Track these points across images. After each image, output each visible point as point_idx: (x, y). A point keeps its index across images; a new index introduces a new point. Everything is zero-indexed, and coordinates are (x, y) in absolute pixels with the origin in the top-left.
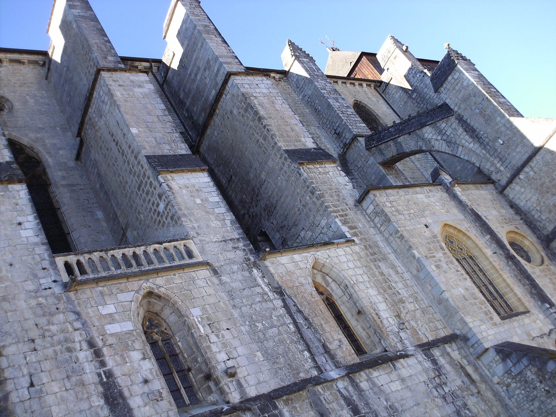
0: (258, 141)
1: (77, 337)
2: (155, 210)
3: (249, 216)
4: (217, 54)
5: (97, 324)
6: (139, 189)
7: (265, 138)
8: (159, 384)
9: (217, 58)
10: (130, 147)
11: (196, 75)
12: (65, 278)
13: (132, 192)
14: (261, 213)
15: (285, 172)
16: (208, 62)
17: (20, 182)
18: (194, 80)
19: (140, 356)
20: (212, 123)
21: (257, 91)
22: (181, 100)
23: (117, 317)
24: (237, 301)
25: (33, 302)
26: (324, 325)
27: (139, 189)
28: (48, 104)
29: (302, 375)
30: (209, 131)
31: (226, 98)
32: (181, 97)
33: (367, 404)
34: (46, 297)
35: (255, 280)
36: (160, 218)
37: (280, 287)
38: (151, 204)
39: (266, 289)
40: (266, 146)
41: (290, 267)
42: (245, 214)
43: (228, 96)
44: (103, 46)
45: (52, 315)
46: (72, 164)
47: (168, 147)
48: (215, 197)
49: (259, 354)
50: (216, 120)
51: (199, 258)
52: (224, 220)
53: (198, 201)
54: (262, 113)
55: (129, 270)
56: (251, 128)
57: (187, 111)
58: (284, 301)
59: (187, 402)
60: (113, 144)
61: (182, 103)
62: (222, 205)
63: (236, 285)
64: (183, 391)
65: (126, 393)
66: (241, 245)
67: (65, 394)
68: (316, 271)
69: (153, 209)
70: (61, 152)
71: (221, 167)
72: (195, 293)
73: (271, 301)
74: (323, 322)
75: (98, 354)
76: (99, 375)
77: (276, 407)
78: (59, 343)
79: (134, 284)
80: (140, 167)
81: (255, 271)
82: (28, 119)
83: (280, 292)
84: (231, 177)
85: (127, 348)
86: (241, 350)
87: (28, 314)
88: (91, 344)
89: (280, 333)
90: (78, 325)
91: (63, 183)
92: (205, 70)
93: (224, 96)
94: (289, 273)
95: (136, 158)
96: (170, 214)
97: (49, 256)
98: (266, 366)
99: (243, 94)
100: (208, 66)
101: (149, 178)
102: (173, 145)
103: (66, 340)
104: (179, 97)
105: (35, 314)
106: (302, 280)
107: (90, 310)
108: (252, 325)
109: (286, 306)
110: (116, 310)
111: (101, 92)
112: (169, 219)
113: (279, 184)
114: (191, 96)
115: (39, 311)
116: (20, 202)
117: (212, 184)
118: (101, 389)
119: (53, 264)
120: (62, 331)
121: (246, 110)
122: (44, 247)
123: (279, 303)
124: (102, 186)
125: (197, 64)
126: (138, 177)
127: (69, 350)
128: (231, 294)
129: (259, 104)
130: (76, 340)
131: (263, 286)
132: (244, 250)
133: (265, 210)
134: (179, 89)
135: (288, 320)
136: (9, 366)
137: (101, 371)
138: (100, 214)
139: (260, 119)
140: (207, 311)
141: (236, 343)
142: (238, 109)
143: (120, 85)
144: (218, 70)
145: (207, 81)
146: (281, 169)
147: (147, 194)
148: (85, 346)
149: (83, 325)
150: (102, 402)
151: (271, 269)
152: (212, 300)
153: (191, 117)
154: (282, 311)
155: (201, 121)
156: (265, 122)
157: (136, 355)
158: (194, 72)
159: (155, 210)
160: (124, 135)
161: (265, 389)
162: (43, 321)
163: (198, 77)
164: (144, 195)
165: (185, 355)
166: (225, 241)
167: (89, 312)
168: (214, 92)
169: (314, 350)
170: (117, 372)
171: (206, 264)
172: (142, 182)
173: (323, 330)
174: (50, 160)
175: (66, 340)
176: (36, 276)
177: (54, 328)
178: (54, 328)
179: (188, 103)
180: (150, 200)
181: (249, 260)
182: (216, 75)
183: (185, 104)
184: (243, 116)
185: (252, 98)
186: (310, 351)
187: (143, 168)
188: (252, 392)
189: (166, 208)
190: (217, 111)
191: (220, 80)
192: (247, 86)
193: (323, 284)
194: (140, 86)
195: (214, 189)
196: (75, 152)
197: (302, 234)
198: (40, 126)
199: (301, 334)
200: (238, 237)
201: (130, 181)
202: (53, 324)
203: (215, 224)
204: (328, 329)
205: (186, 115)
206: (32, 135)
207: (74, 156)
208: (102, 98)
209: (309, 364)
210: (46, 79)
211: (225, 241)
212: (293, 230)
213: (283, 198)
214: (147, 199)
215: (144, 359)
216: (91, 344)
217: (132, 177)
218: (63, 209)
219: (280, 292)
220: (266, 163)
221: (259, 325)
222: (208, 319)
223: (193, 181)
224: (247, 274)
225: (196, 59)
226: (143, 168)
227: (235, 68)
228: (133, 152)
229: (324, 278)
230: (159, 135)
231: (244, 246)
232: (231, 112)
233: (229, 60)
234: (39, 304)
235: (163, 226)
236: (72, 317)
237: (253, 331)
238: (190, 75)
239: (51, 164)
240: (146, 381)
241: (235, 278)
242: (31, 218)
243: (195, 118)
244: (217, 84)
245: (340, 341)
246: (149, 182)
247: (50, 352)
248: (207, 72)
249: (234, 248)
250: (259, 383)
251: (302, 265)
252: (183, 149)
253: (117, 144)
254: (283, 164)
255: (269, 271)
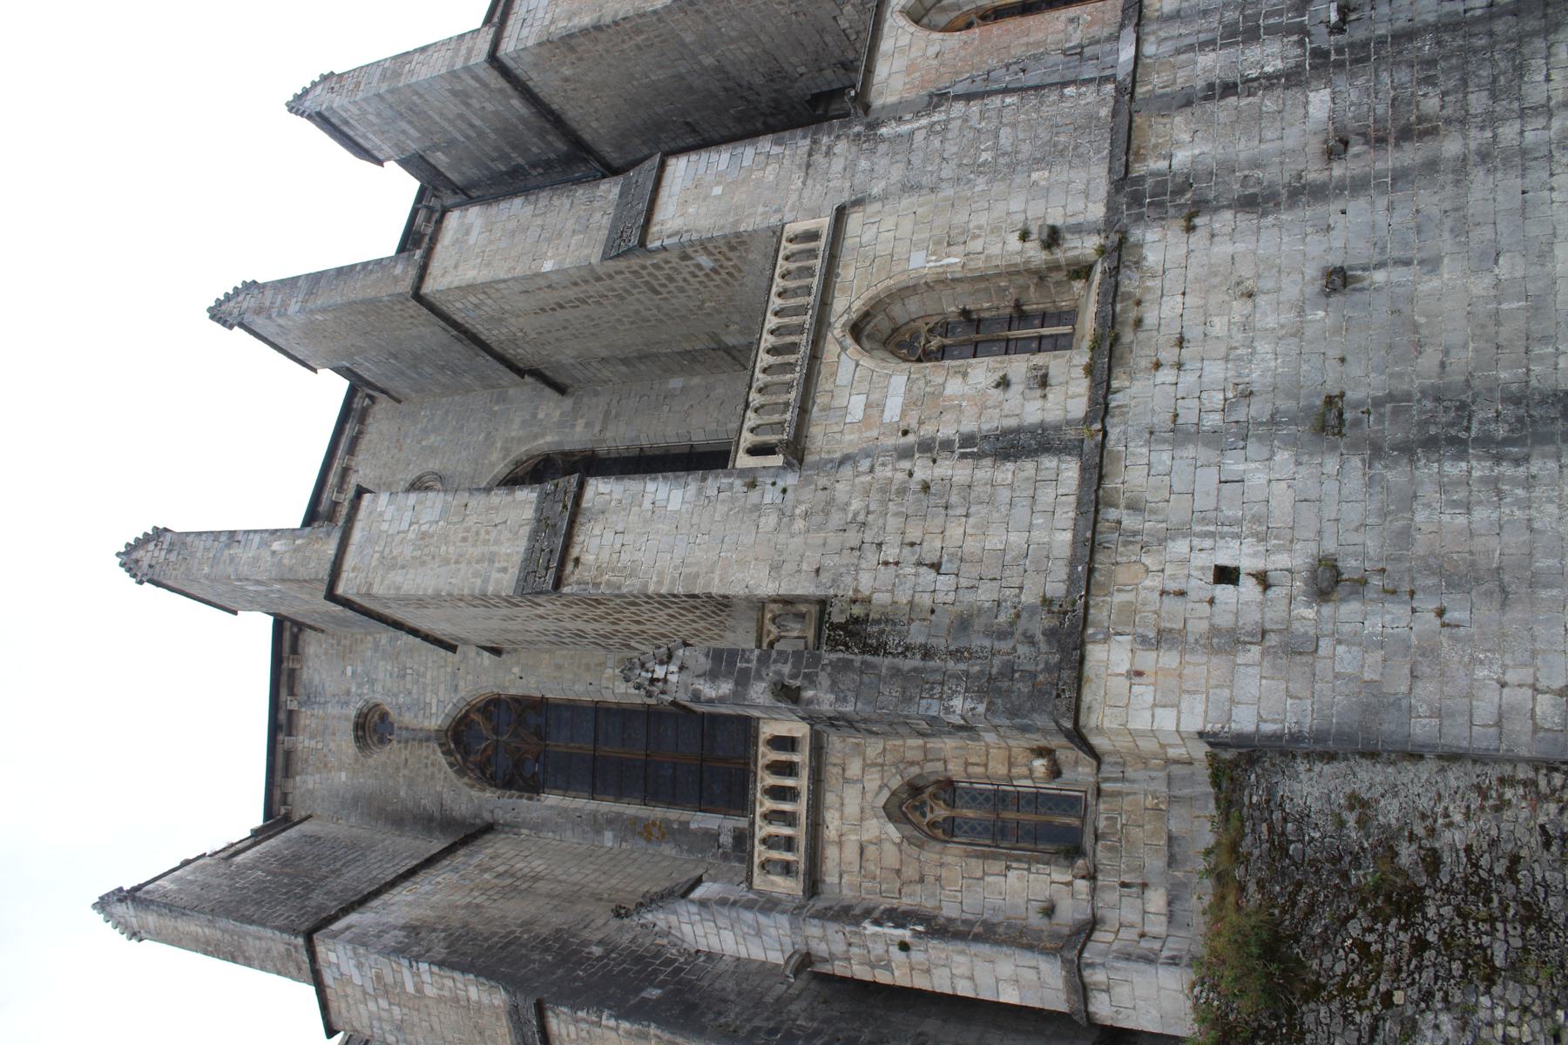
0: (638, 47)
1: (884, 473)
2: (707, 275)
3: (772, 115)
4: (444, 71)
5: (875, 433)
6: (658, 293)
7: (638, 31)
8: (1019, 366)
9: (453, 74)
10: (575, 284)
11: (472, 126)
12: (777, 460)
13: (659, 308)
14: (776, 91)
15: (716, 13)
16: (455, 93)
17: (581, 486)
18: (481, 134)
19: (959, 380)
20: (574, 125)
21: (540, 14)
22: (507, 173)
23: (875, 396)
24: (925, 180)
25: (799, 524)
26: (1031, 40)
27: (658, 293)
28: (447, 413)
29: (1104, 112)
30: (587, 136)
31: (538, 81)
32: (503, 169)
33: (1205, 13)
34: (799, 502)
35: (900, 135)
36: (723, 272)
37: (931, 96)
38: (692, 280)
39: (924, 121)
40: (652, 35)
41: (900, 63)
42: (765, 123)
43: (534, 75)
44: (374, 277)
45: (830, 502)
46: (568, 403)
47: (598, 215)
48: (721, 159)
49: (1035, 176)
50: (572, 114)
51: (824, 223)
52: (768, 155)
53: (718, 191)
54: (586, 20)
55: (804, 350)
56: (608, 51)
57: (534, 166)
58: (957, 97)
59: (1067, 329)
60: (559, 313)
61: (516, 172)
62: (740, 150)
63: (897, 173)
64: (1046, 331)
65: (1012, 422)
66: (825, 140)
67: (971, 520)
68: (925, 21)
69: (703, 279)
70: (541, 416)
71: (663, 136)
72: (883, 249)
73: (948, 121)
74: (1025, 40)
75: (926, 447)
76: (963, 456)
77: (1142, 178)
78: (884, 503)
79: (831, 349)
80: (618, 277)
81: (883, 130)
82: (464, 454)
83: (938, 99)
84: (687, 124)
85: (937, 395)
86: (1016, 204)
87: (817, 538)
88: (905, 453)
89: (1013, 125)
90: (865, 465)
91: (597, 428)
92: (468, 105)
93: (530, 84)
94: (910, 69)
95: (599, 279)
96: (725, 249)
97: (727, 476)
98: (1062, 173)
99: (540, 45)
100: (462, 96)
101: (644, 267)
102: (596, 204)
103: (883, 490)
104: (502, 174)
105: (821, 527)
106: (932, 51)
107: (847, 438)
108: (979, 169)
109: (968, 97)
110: (866, 396)
111: (459, 305)
112: (731, 254)
113: (733, 34)
114: (508, 150)
115: (819, 518)
116: (616, 496)
117: (694, 157)
118: (988, 462)
119: (743, 473)
120: (867, 493)
121: (572, 49)
122: (710, 481)
123: (959, 108)
124: (625, 361)
125: (451, 116)
126: (635, 286)
127: (902, 491)
128: (909, 188)
129: (570, 20)
130: (889, 474)
131: (916, 125)
132: (838, 137)
133: (772, 80)
134: (488, 168)
135: (996, 101)
136: (892, 591)
137: (958, 451)
138: (675, 383)
139: (598, 28)
140: (923, 241)
141: (1000, 209)
142: (563, 64)
143: (456, 267)
144: (477, 78)
145: (490, 107)
146: (707, 19)
147: (670, 279)
148: (906, 464)
149: (868, 456)
150: (1010, 466)
151: (891, 99)
152: (907, 225)
153: (548, 165)
154: (975, 107)
155: (561, 146)
156: (608, 20)
157: (954, 386)
158: (464, 126)
159: (707, 275)
160: (549, 287)
161: (1102, 187)
162: (836, 518)
163: (477, 122)
164: (672, 287)
165: (986, 305)
166: (808, 166)
167: (850, 441)
168: (516, 103)
169: (1070, 76)
170: (969, 426)
171: (841, 214)
172: (647, 283)
173: (1038, 44)
174: (549, 439)
175: (883, 490)
176: (757, 508)
177: (856, 504)
178: (856, 504)
179: (521, 161)
180: (685, 280)
181: (858, 135)
182: (486, 86)
183: (519, 166)
184: (580, 59)
185: (552, 29)
186: (1065, 84)
187: (621, 272)
188: (1097, 211)
189: (710, 254)
190: (555, 107)
191: (496, 81)
192: (525, 32)
193: (953, 15)
194: (468, 232)
195: (704, 155)
196: (548, 391)
197: (843, 24)
198: (482, 436)
199: (1030, 88)
200: (808, 141)
201: (637, 306)
202: (848, 504)
203: (770, 173)
204: (1040, 36)
205: (540, 170)
206: (495, 456)
207: (556, 396)
208: (470, 306)
209: (1090, 94)
210: (399, 402)
211: (808, 166)
212: (828, 38)
213: (763, 37)
214: (682, 284)
215: (965, 375)
216: (905, 453)
217: (630, 299)
218: (645, 442)
219: (938, 99)
220: (684, 45)
221: (985, 156)
222: (938, 243)
223: (676, 189)
224: (883, 148)
225: (441, 114)
226: (621, 272)
227: (484, 46)
228: (586, 282)
229: (944, 10)
230: (570, 224)
231: (829, 135)
232: (566, 80)
233: (463, 51)
234: (806, 515)
235: (740, 270)
236: (847, 470)
237: (989, 170)
238: (468, 137)
239: (556, 438)
240: (1004, 383)
241: (882, 171)
242: (651, 486)
243: (552, 156)
244: (501, 91)
245: (1072, 20)
246: (651, 269)
247: (893, 523)
248: (473, 102)
249: (827, 154)
250: (1086, 194)
251: (904, 40)
252: (610, 190)
253: (561, 307)
254: (699, 11)
255: (893, 105)
